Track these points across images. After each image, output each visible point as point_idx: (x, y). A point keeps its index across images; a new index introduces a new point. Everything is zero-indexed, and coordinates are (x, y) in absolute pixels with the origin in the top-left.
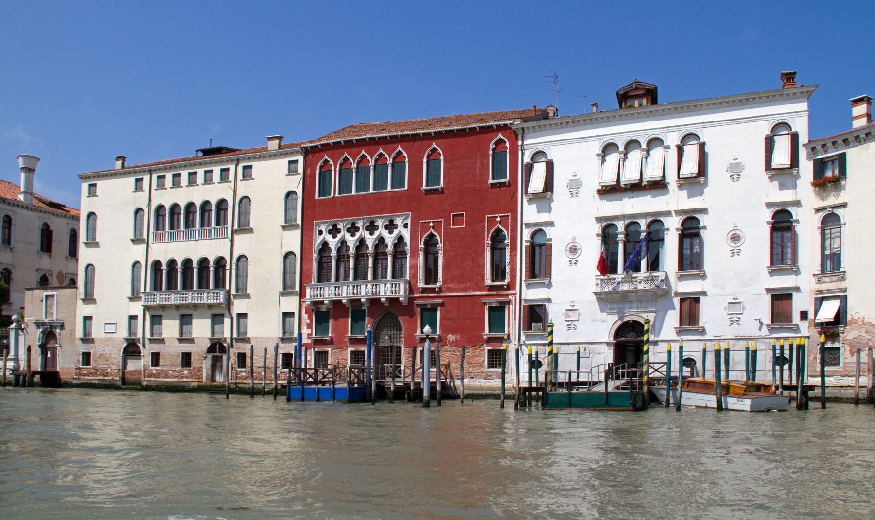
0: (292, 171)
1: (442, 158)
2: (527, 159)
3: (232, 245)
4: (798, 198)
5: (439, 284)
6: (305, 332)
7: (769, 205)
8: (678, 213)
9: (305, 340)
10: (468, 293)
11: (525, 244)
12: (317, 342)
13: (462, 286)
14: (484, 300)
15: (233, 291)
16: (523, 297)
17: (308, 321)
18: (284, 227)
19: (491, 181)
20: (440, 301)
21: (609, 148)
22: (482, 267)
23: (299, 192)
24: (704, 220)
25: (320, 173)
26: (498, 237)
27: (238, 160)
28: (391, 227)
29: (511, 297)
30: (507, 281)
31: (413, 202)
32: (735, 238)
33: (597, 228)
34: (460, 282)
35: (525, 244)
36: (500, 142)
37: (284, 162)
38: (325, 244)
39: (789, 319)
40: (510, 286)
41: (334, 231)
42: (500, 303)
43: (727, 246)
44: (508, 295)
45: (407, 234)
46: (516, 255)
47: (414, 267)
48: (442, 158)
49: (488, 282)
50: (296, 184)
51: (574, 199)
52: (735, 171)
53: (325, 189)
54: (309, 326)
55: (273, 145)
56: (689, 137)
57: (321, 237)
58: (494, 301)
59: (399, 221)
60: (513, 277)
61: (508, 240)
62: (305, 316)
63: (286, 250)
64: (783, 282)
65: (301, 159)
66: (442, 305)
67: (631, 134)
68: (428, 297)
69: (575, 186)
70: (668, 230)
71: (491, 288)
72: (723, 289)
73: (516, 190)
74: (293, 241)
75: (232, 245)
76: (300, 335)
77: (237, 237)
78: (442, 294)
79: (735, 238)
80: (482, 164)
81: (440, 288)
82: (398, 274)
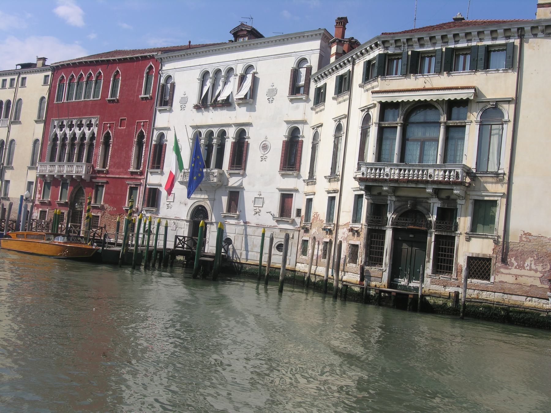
0: (45, 83)
1: (120, 78)
2: (162, 81)
3: (9, 131)
4: (306, 118)
5: (107, 168)
6: (38, 196)
7: (288, 122)
8: (237, 125)
9: (37, 202)
10: (120, 176)
11: (154, 143)
12: (43, 203)
13: (118, 170)
14: (128, 182)
15: (5, 165)
16: (148, 181)
17: (40, 189)
18: (36, 122)
19: (143, 96)
20: (104, 180)
21: (205, 74)
22: (129, 157)
23: (47, 97)
24: (250, 132)
25: (59, 85)
26: (141, 136)
27: (20, 73)
28: (90, 126)
29: (142, 181)
30: (141, 169)
31: (103, 108)
32: (265, 147)
33: (191, 132)
34: (118, 168)
35: (154, 143)
36: (151, 68)
37: (41, 76)
38: (56, 135)
39: (289, 215)
40: (142, 173)
41: (61, 127)
42: (136, 185)
43: (260, 153)
44: (140, 179)
45: (96, 130)
46: (148, 151)
47: (96, 155)
48: (120, 78)
49: (132, 169)
50: (44, 91)
51: (183, 112)
52: (272, 93)
53: (59, 98)
54: (40, 193)
55: (40, 63)
56: (249, 67)
57: (54, 130)
58: (132, 183)
59: (93, 121)
60: (144, 167)
61: (145, 140)
62: (39, 185)
63: (35, 138)
64: (289, 183)
65: (50, 73)
66: (107, 183)
67: (217, 65)
68: (100, 177)
69: (184, 101)
70: (228, 138)
71: (132, 173)
72: (254, 186)
73: (154, 103)
74: (38, 130)
75: (9, 131)
76: (35, 196)
77: (12, 126)
78: (108, 176)
79: (265, 147)
80: (139, 83)
81: (107, 171)
82: (89, 160)
